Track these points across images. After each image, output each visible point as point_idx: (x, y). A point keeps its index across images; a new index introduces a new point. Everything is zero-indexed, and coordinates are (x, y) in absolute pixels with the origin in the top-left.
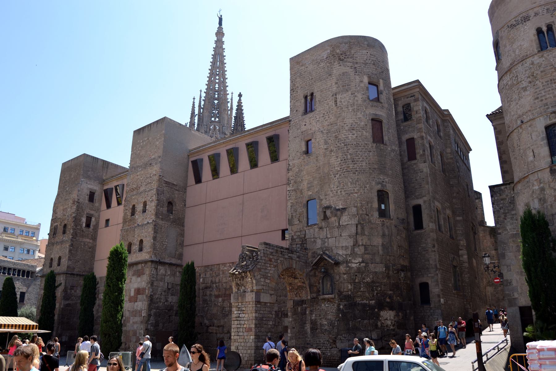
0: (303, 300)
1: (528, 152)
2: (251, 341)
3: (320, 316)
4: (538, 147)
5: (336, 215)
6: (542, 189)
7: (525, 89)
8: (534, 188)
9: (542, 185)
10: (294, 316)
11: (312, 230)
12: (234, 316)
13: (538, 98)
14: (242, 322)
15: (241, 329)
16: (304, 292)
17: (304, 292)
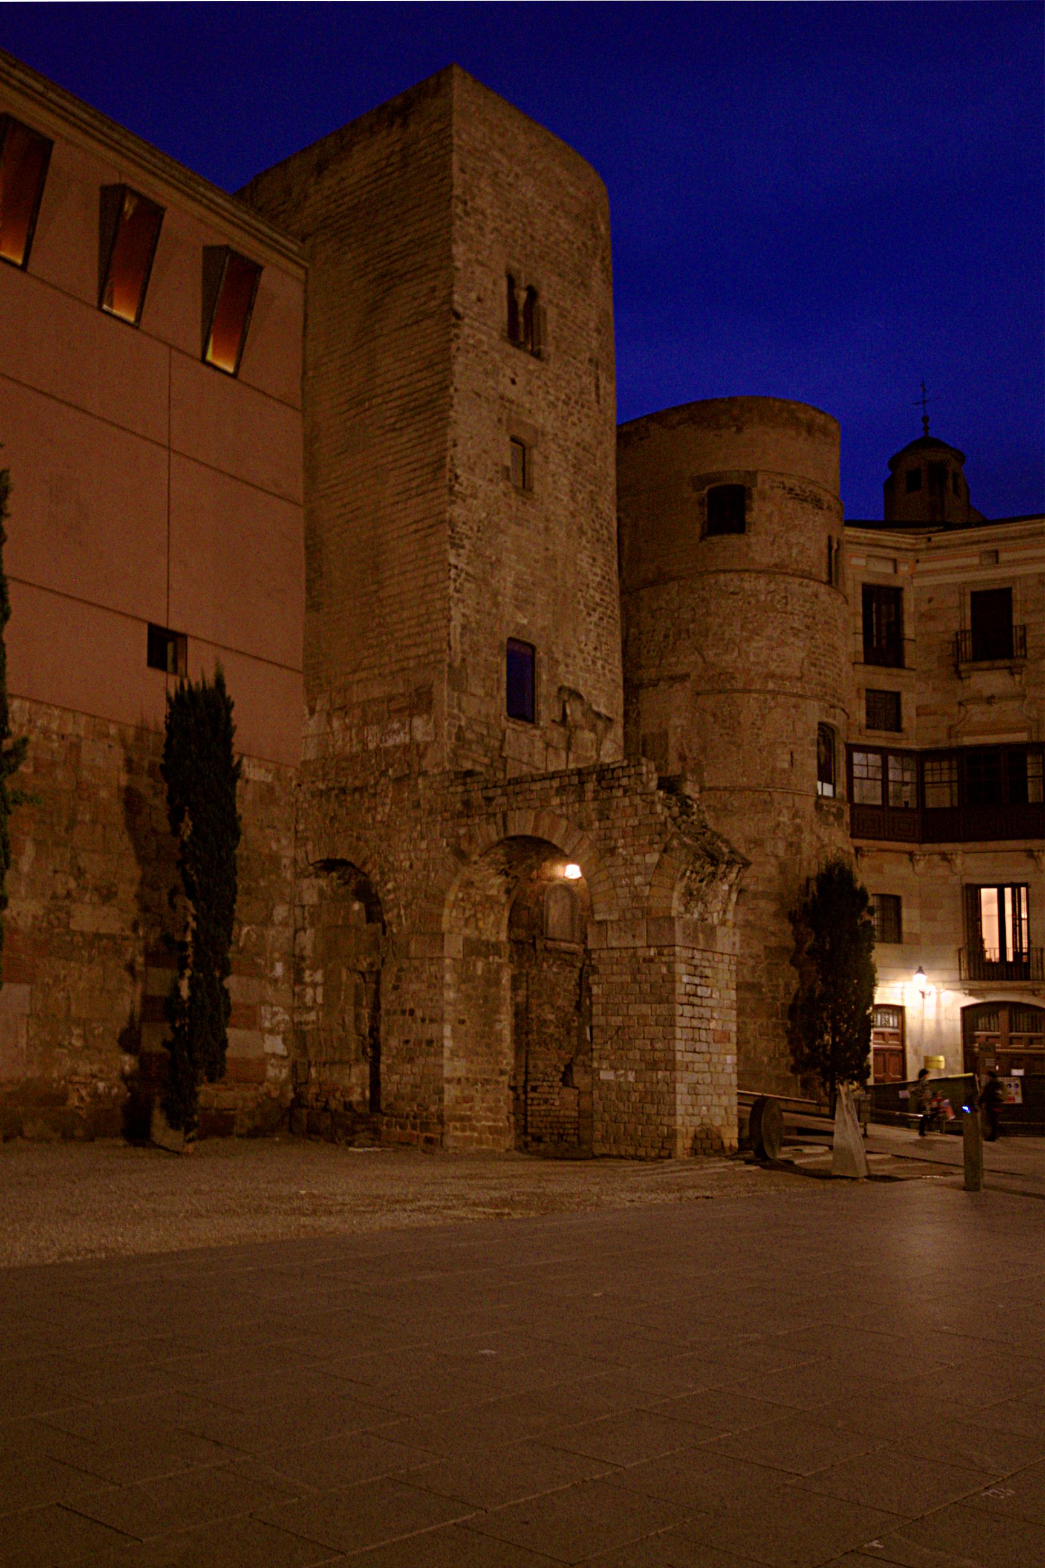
0: (487, 943)
1: (779, 752)
2: (729, 1069)
3: (540, 996)
4: (803, 752)
5: (593, 728)
6: (798, 829)
7: (796, 632)
8: (781, 819)
9: (798, 821)
10: (463, 987)
11: (524, 739)
12: (680, 989)
13: (815, 665)
14: (707, 1013)
15: (703, 1033)
16: (492, 918)
17: (492, 918)
